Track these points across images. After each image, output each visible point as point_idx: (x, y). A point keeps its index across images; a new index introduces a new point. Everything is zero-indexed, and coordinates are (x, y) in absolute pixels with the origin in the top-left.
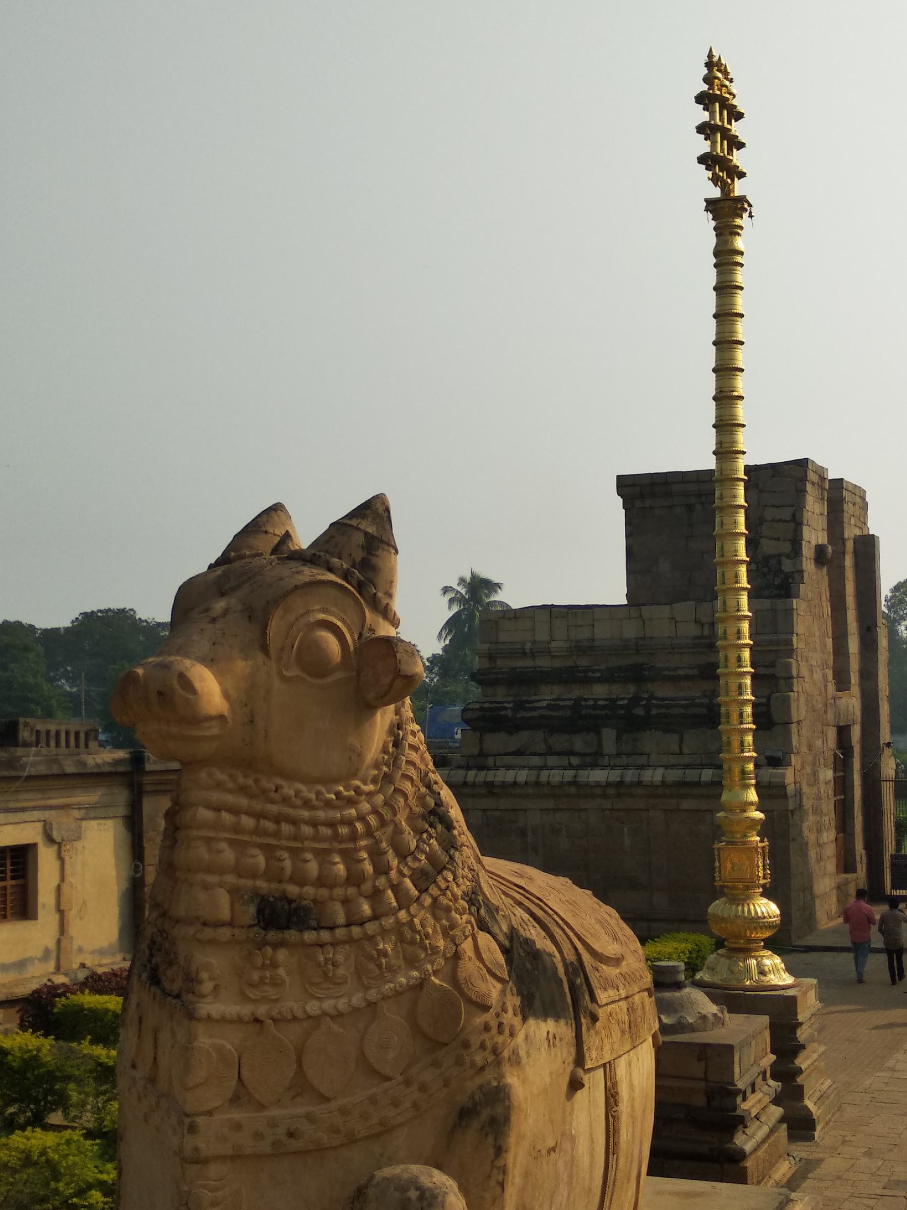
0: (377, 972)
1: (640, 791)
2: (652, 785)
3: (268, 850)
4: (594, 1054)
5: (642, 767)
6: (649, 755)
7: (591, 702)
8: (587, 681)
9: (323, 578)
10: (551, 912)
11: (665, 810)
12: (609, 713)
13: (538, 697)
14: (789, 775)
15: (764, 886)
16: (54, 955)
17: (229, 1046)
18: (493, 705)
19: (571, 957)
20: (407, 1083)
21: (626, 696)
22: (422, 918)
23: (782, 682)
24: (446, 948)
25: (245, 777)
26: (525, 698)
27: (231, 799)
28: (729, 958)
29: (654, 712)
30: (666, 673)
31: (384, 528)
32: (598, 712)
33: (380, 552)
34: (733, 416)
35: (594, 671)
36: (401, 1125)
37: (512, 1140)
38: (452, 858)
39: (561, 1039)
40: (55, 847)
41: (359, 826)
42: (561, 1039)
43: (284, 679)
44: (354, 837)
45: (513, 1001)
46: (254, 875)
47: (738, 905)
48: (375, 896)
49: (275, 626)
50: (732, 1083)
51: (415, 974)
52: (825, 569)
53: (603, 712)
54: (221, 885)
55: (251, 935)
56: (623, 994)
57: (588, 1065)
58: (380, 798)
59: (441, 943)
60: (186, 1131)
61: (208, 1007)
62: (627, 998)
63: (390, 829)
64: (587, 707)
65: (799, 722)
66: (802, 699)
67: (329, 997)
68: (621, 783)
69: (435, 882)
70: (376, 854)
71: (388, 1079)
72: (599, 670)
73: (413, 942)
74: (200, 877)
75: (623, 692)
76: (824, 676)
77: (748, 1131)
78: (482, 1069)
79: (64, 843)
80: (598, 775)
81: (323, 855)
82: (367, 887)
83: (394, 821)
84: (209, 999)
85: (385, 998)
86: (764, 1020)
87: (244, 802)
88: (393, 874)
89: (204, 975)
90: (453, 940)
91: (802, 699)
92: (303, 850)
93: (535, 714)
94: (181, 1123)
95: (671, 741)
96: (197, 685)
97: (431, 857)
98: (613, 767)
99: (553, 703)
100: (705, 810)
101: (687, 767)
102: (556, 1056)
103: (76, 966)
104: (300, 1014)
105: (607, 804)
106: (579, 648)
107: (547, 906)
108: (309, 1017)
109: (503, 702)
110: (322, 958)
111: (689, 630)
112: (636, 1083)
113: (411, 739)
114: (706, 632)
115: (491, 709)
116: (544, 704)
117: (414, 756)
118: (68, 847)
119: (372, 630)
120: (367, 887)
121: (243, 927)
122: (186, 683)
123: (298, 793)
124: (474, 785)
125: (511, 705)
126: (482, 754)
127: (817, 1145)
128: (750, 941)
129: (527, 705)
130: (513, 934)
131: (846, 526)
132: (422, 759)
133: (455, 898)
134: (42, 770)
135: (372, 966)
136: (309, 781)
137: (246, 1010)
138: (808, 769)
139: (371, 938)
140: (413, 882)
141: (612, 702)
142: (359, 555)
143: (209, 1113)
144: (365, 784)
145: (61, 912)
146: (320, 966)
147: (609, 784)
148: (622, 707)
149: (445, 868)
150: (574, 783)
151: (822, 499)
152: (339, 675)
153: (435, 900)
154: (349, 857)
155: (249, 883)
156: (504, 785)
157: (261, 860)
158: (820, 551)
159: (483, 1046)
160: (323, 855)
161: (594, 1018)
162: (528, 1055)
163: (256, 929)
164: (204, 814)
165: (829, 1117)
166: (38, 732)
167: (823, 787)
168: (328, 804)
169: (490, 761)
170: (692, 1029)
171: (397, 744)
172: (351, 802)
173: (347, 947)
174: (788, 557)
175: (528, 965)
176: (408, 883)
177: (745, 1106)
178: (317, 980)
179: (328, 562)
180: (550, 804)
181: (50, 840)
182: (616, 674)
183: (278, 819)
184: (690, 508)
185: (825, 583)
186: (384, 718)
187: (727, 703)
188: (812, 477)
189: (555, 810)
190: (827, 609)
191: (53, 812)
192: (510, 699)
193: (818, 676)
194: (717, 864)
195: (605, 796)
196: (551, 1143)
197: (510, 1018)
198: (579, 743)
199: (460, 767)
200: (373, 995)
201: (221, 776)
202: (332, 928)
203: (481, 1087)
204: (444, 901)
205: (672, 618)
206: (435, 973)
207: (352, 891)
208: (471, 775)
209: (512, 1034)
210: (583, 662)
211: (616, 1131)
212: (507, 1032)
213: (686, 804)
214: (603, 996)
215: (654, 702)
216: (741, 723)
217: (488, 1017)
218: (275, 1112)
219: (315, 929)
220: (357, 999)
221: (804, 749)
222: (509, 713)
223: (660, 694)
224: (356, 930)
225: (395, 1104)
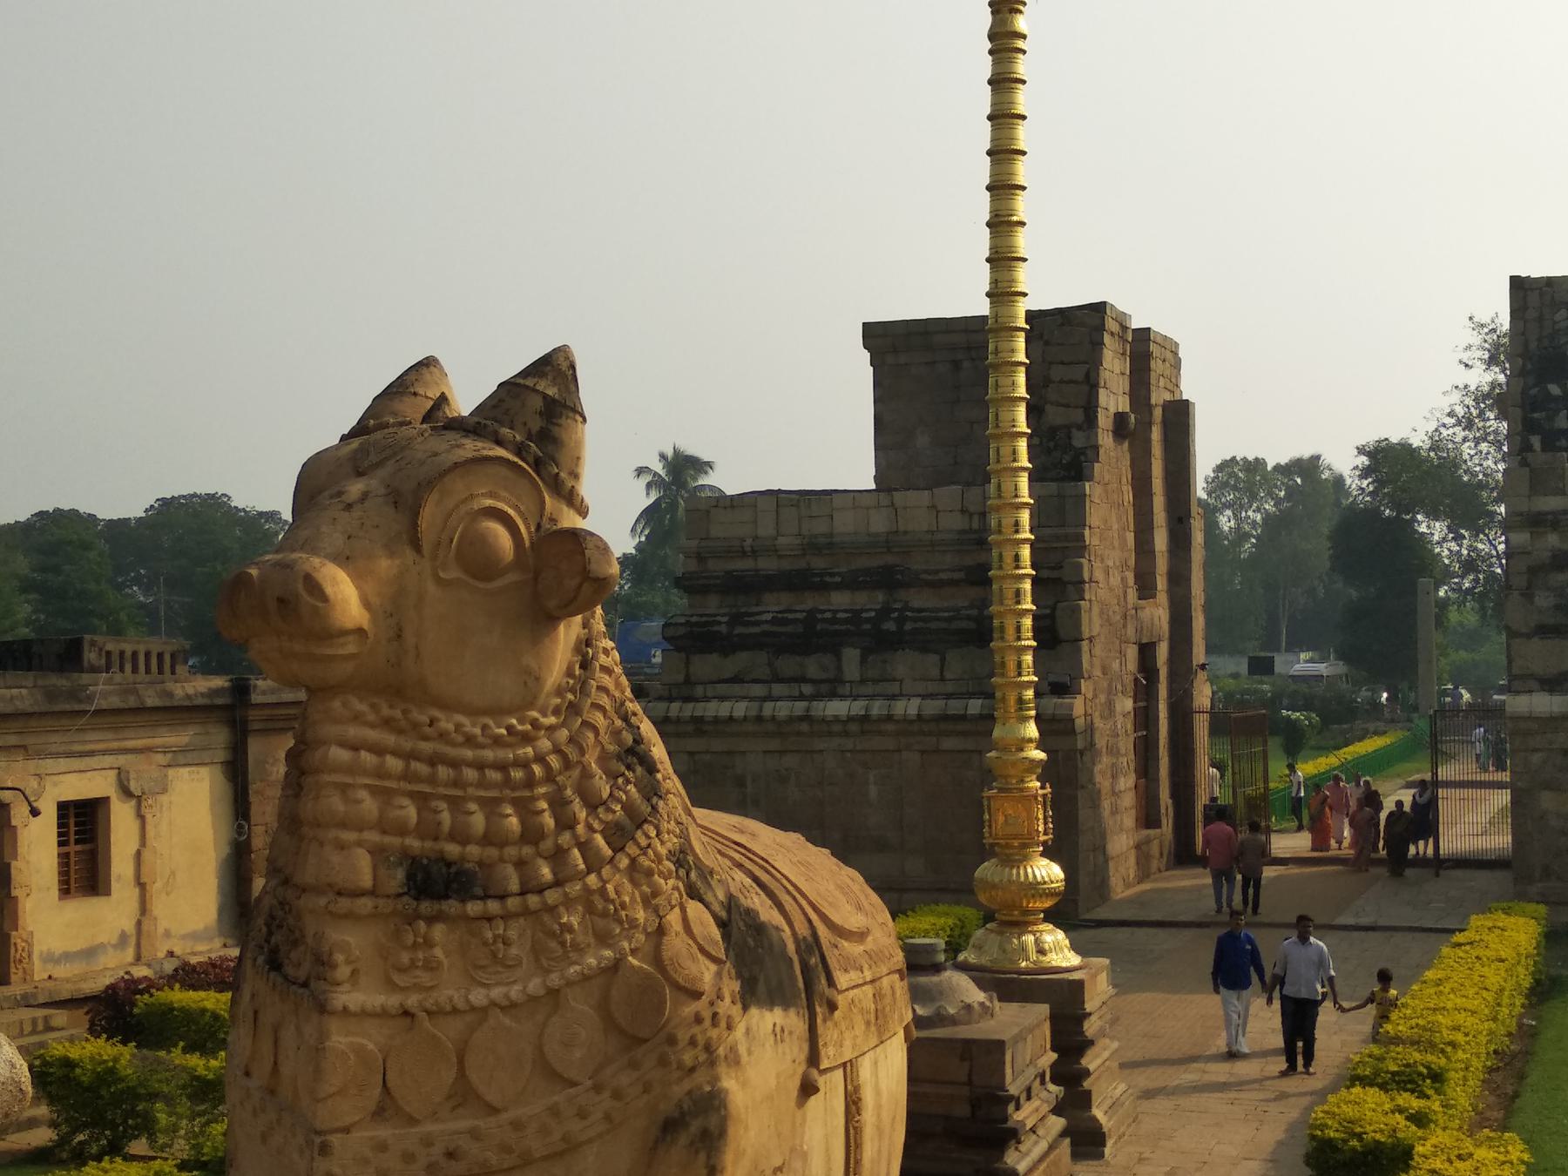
0: (560, 951)
1: (890, 727)
2: (905, 720)
3: (422, 799)
4: (831, 1051)
5: (893, 697)
6: (901, 681)
7: (828, 615)
8: (824, 587)
9: (491, 453)
10: (779, 876)
11: (923, 752)
12: (852, 628)
13: (760, 609)
14: (1078, 706)
15: (1044, 843)
16: (133, 941)
17: (371, 1046)
18: (704, 619)
19: (803, 930)
20: (598, 1088)
21: (873, 607)
22: (617, 883)
23: (1070, 588)
24: (646, 920)
25: (391, 707)
26: (743, 610)
27: (372, 735)
28: (1001, 933)
29: (908, 626)
30: (924, 576)
31: (567, 388)
32: (837, 627)
33: (562, 421)
34: (1011, 248)
35: (832, 575)
36: (590, 1141)
37: (728, 1158)
38: (654, 808)
39: (791, 1033)
40: (133, 802)
41: (537, 769)
42: (791, 1033)
43: (439, 581)
44: (530, 782)
45: (732, 986)
46: (402, 831)
47: (1012, 867)
48: (558, 856)
49: (429, 515)
50: (1003, 1088)
51: (608, 953)
52: (1126, 445)
53: (843, 627)
54: (359, 844)
55: (400, 907)
56: (868, 975)
57: (824, 1065)
58: (563, 734)
59: (641, 915)
60: (316, 1152)
61: (348, 997)
62: (872, 981)
63: (576, 773)
64: (824, 620)
65: (1091, 639)
66: (1096, 610)
67: (498, 984)
68: (865, 719)
69: (633, 838)
70: (559, 804)
71: (573, 1084)
72: (838, 574)
73: (604, 914)
74: (333, 833)
75: (868, 601)
76: (1124, 580)
77: (1023, 1148)
78: (692, 1070)
79: (144, 797)
80: (837, 708)
81: (491, 806)
82: (547, 845)
83: (579, 762)
84: (346, 987)
85: (570, 984)
86: (1044, 1009)
87: (390, 739)
88: (580, 829)
89: (339, 957)
90: (656, 910)
91: (1096, 610)
92: (464, 799)
94: (310, 1143)
96: (329, 590)
97: (628, 808)
98: (856, 698)
99: (780, 615)
100: (972, 751)
101: (949, 696)
102: (784, 1053)
103: (161, 954)
104: (461, 1005)
105: (849, 744)
106: (813, 546)
107: (773, 867)
108: (473, 1009)
109: (715, 615)
110: (489, 935)
111: (954, 522)
112: (883, 1086)
113: (603, 659)
114: (975, 525)
115: (697, 624)
116: (768, 617)
117: (607, 681)
118: (150, 802)
119: (553, 520)
120: (547, 845)
121: (388, 896)
122: (314, 587)
123: (458, 727)
124: (678, 720)
125: (725, 619)
126: (688, 681)
127: (1108, 1164)
128: (1027, 912)
129: (746, 619)
130: (731, 903)
131: (1153, 388)
132: (618, 684)
133: (659, 860)
134: (115, 702)
135: (553, 944)
136: (473, 712)
137: (393, 1001)
138: (1102, 698)
139: (552, 910)
140: (605, 838)
141: (856, 614)
142: (536, 424)
143: (346, 1130)
144: (545, 715)
145: (141, 886)
146: (485, 944)
147: (851, 719)
148: (868, 620)
149: (646, 821)
150: (806, 718)
151: (1123, 354)
152: (511, 577)
153: (633, 860)
154: (525, 808)
155: (393, 841)
156: (716, 720)
157: (411, 812)
158: (1120, 418)
159: (693, 1042)
160: (491, 806)
161: (832, 1007)
162: (750, 1053)
163: (406, 899)
164: (339, 754)
165: (1122, 1130)
166: (109, 653)
167: (1120, 720)
168: (497, 742)
169: (699, 691)
170: (953, 1021)
171: (585, 665)
172: (527, 739)
173: (522, 920)
174: (1079, 428)
175: (751, 942)
176: (599, 839)
177: (1019, 1116)
178: (484, 962)
179: (496, 433)
180: (774, 744)
181: (126, 792)
182: (861, 579)
183: (433, 761)
184: (956, 365)
185: (1126, 462)
186: (568, 632)
187: (1001, 615)
188: (1111, 325)
189: (782, 753)
190: (1129, 496)
191: (129, 757)
192: (726, 610)
193: (1115, 580)
194: (987, 817)
195: (846, 734)
196: (778, 1162)
197: (726, 1007)
198: (813, 666)
199: (660, 699)
200: (555, 980)
201: (361, 707)
202: (502, 897)
203: (689, 1093)
204: (644, 862)
205: (934, 507)
206: (633, 952)
207: (527, 850)
208: (675, 706)
209: (729, 1027)
210: (819, 563)
211: (858, 1146)
212: (723, 1024)
213: (949, 743)
214: (843, 980)
215: (909, 614)
216: (1019, 639)
217: (700, 1006)
218: (429, 1127)
219: (481, 898)
220: (535, 985)
221: (1097, 672)
222: (723, 629)
223: (916, 604)
224: (533, 900)
225: (582, 1114)
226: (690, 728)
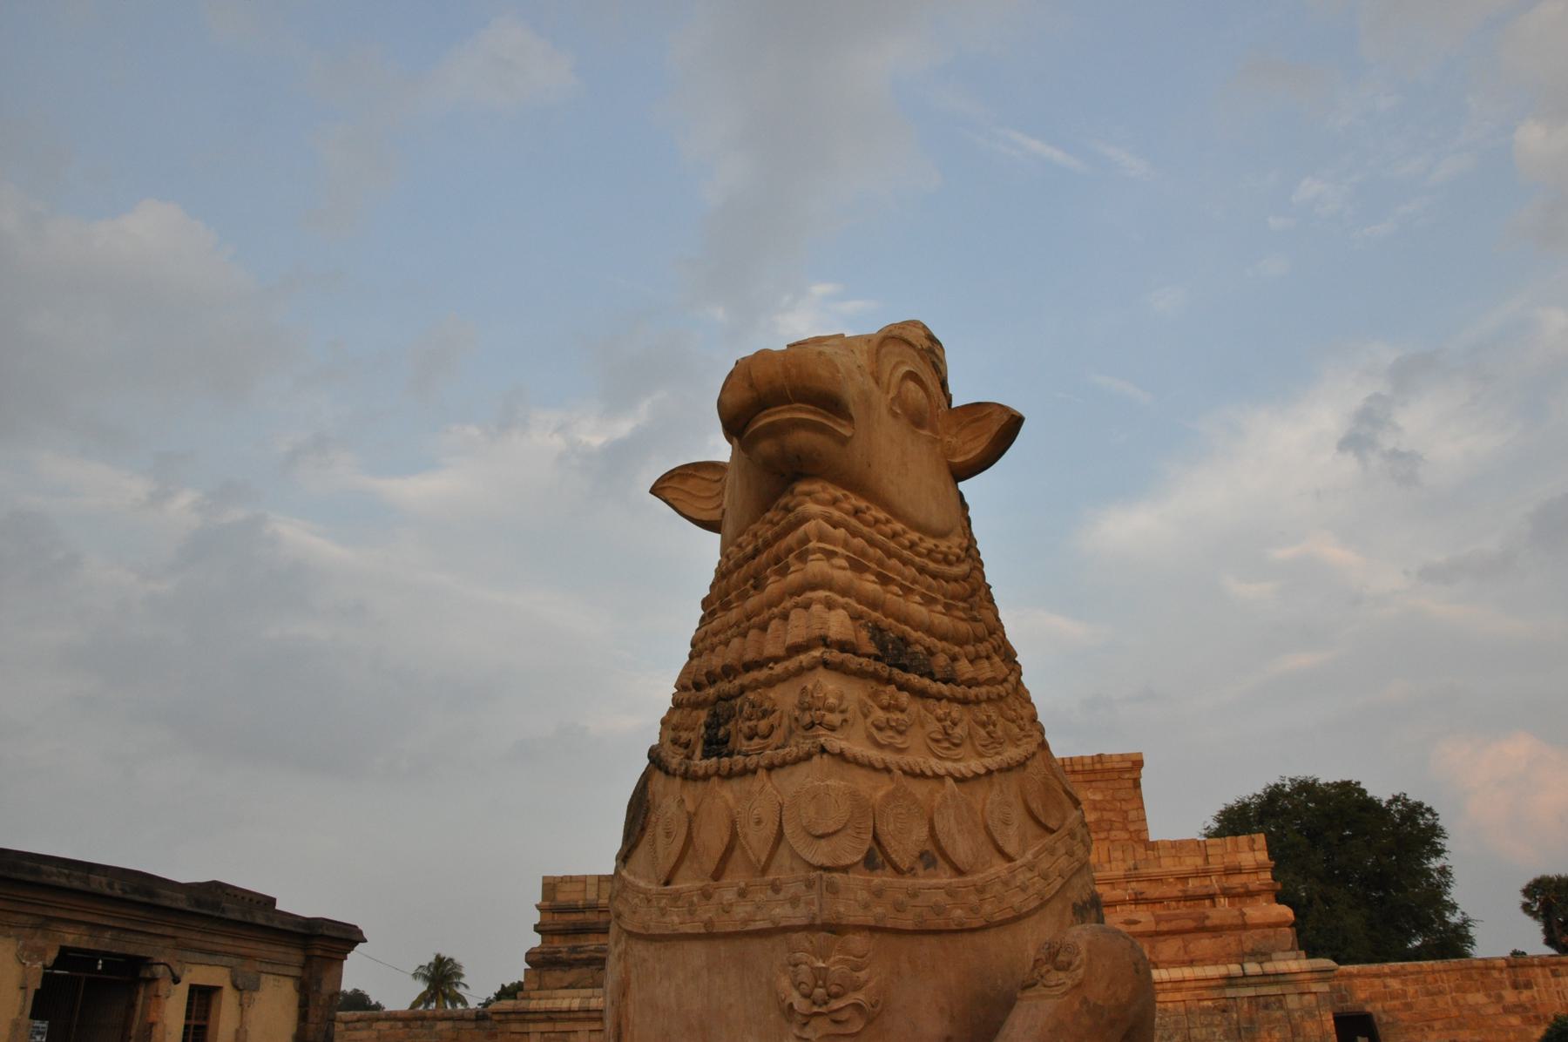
93: (584, 956)
116: (593, 948)
222: (564, 956)
226: (544, 1016)
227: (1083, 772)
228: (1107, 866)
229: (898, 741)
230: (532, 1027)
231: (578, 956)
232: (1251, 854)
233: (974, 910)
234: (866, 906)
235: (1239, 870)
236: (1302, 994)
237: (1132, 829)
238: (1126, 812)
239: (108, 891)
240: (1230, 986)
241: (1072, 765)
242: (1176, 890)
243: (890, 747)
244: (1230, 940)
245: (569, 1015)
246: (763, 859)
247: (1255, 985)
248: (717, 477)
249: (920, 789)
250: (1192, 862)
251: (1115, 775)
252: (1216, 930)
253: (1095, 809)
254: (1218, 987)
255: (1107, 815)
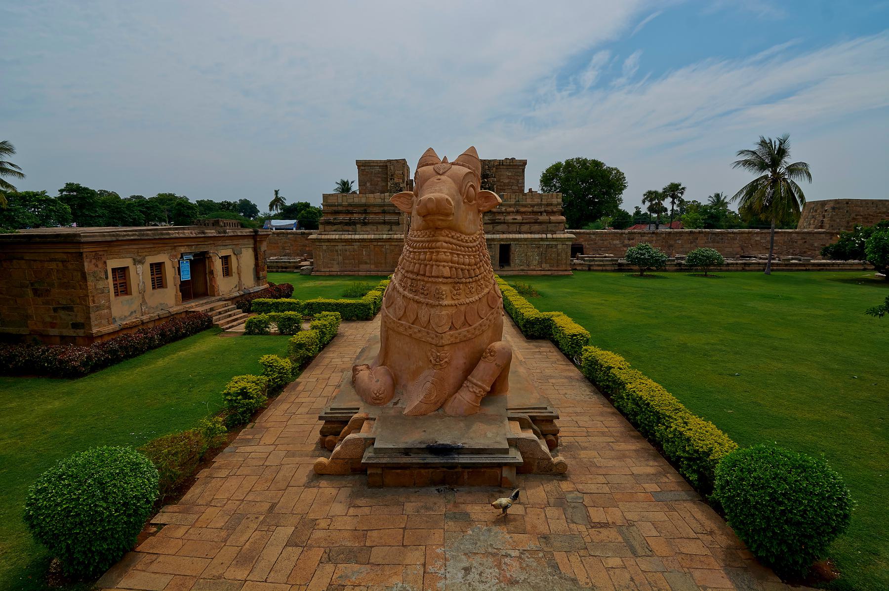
29: (370, 221)
75: (362, 217)
93: (338, 221)
95: (375, 227)
106: (350, 205)
180: (344, 244)
195: (359, 242)
198: (350, 228)
210: (350, 208)
213: (379, 244)
227: (507, 165)
228: (509, 200)
229: (458, 297)
230: (323, 244)
231: (336, 221)
232: (556, 199)
233: (473, 334)
234: (449, 339)
235: (551, 205)
236: (563, 244)
237: (519, 186)
238: (518, 180)
239: (191, 236)
240: (541, 241)
241: (503, 163)
242: (530, 210)
243: (458, 299)
244: (544, 226)
245: (334, 240)
246: (425, 325)
247: (549, 241)
248: (410, 198)
249: (463, 308)
250: (537, 201)
251: (517, 167)
252: (541, 223)
253: (508, 178)
254: (538, 241)
255: (512, 181)
